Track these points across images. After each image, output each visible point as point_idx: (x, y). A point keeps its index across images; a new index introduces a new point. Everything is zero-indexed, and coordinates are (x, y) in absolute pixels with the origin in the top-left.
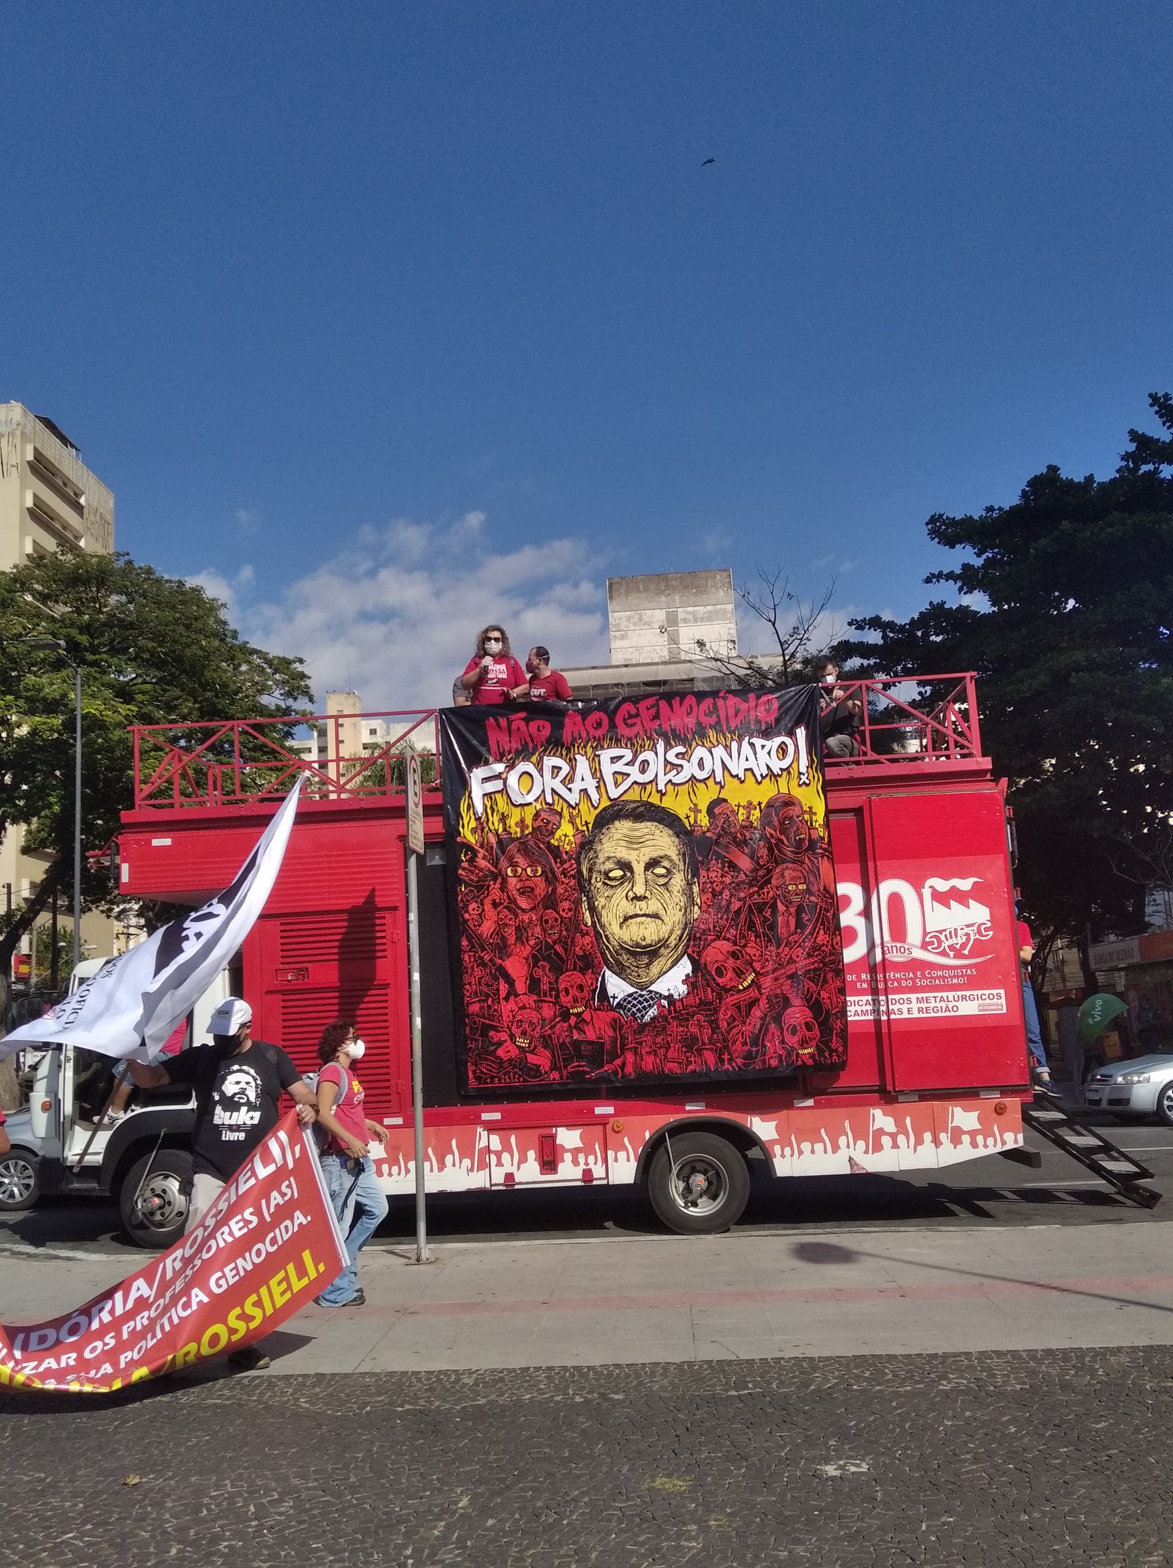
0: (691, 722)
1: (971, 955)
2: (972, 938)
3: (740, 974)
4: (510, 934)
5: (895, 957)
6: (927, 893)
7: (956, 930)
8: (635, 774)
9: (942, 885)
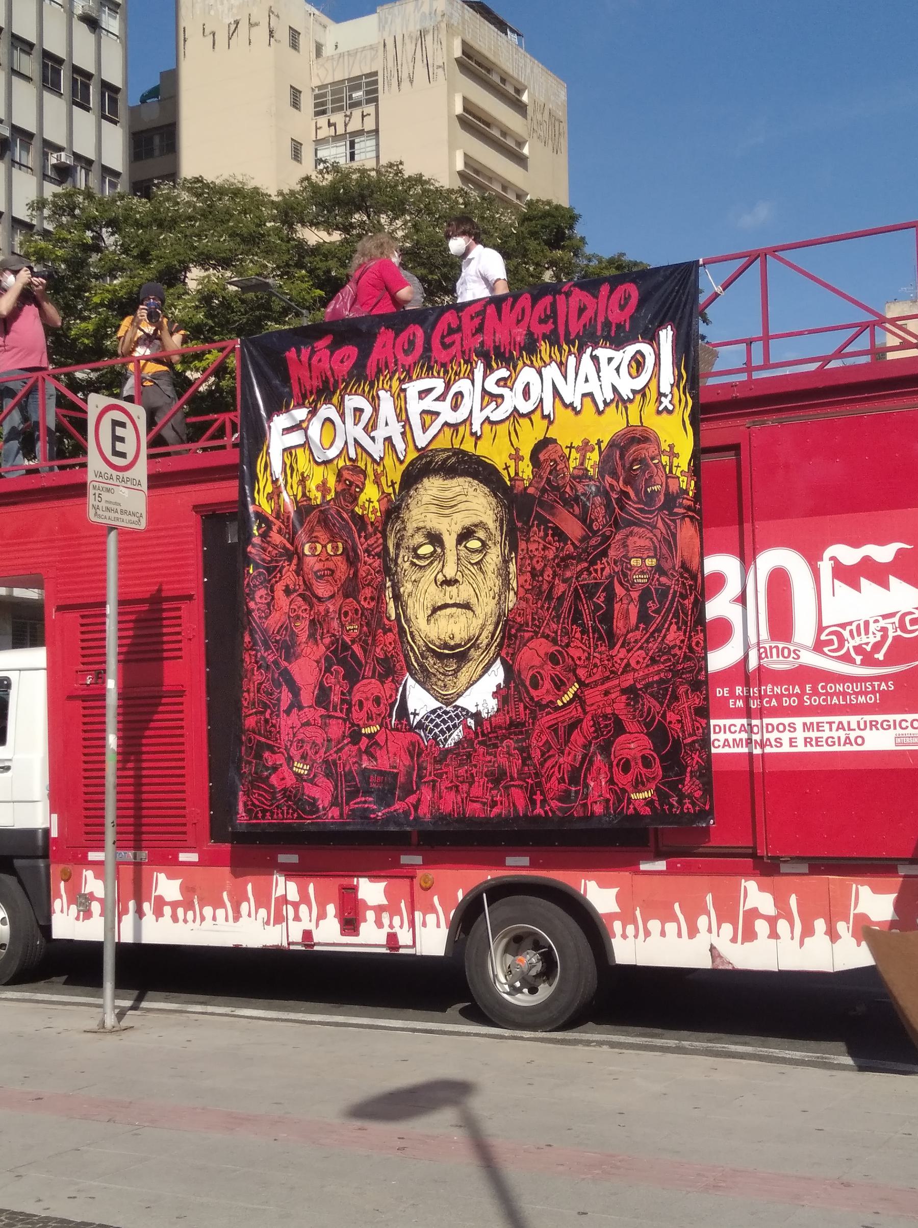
0: (520, 334)
1: (889, 660)
2: (891, 634)
3: (560, 686)
4: (302, 628)
5: (777, 664)
6: (825, 567)
7: (867, 623)
8: (447, 415)
9: (849, 555)
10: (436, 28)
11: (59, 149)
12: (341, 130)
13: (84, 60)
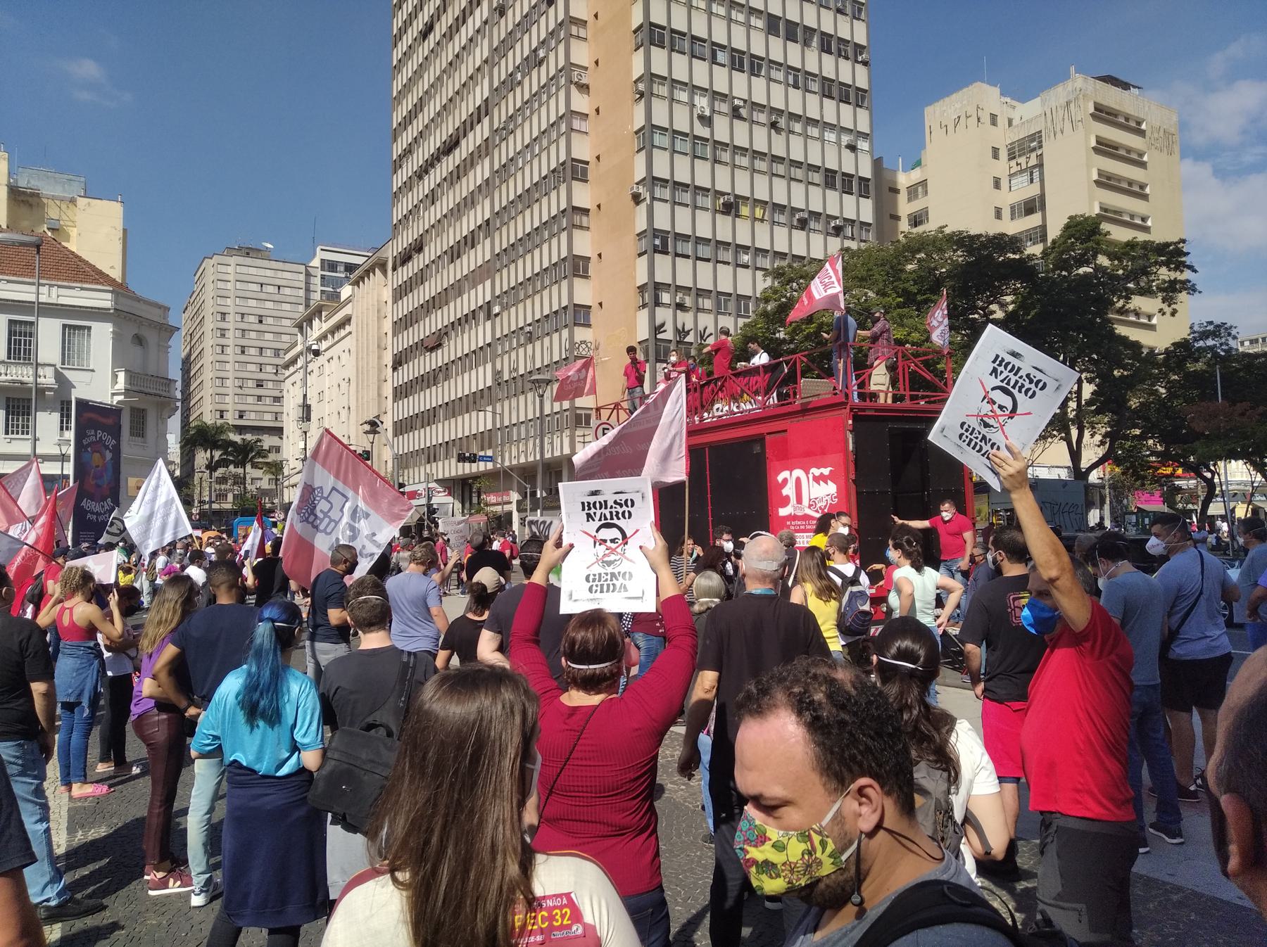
6: (811, 476)
10: (1077, 99)
11: (836, 218)
12: (1024, 167)
13: (848, 168)
